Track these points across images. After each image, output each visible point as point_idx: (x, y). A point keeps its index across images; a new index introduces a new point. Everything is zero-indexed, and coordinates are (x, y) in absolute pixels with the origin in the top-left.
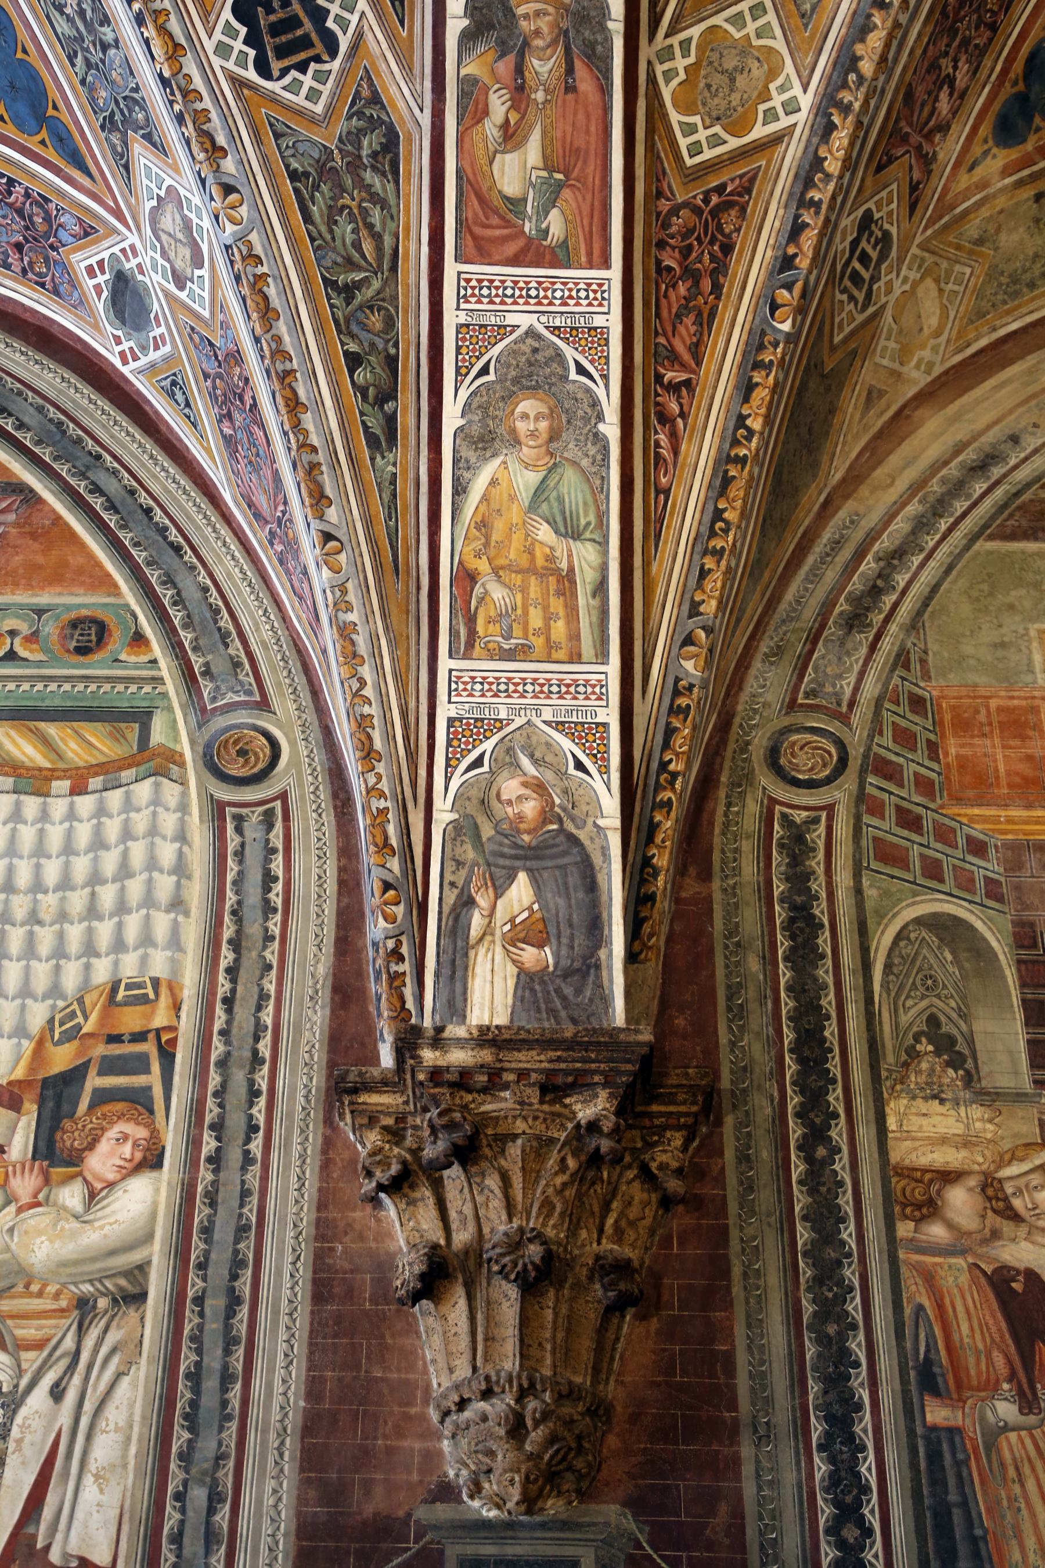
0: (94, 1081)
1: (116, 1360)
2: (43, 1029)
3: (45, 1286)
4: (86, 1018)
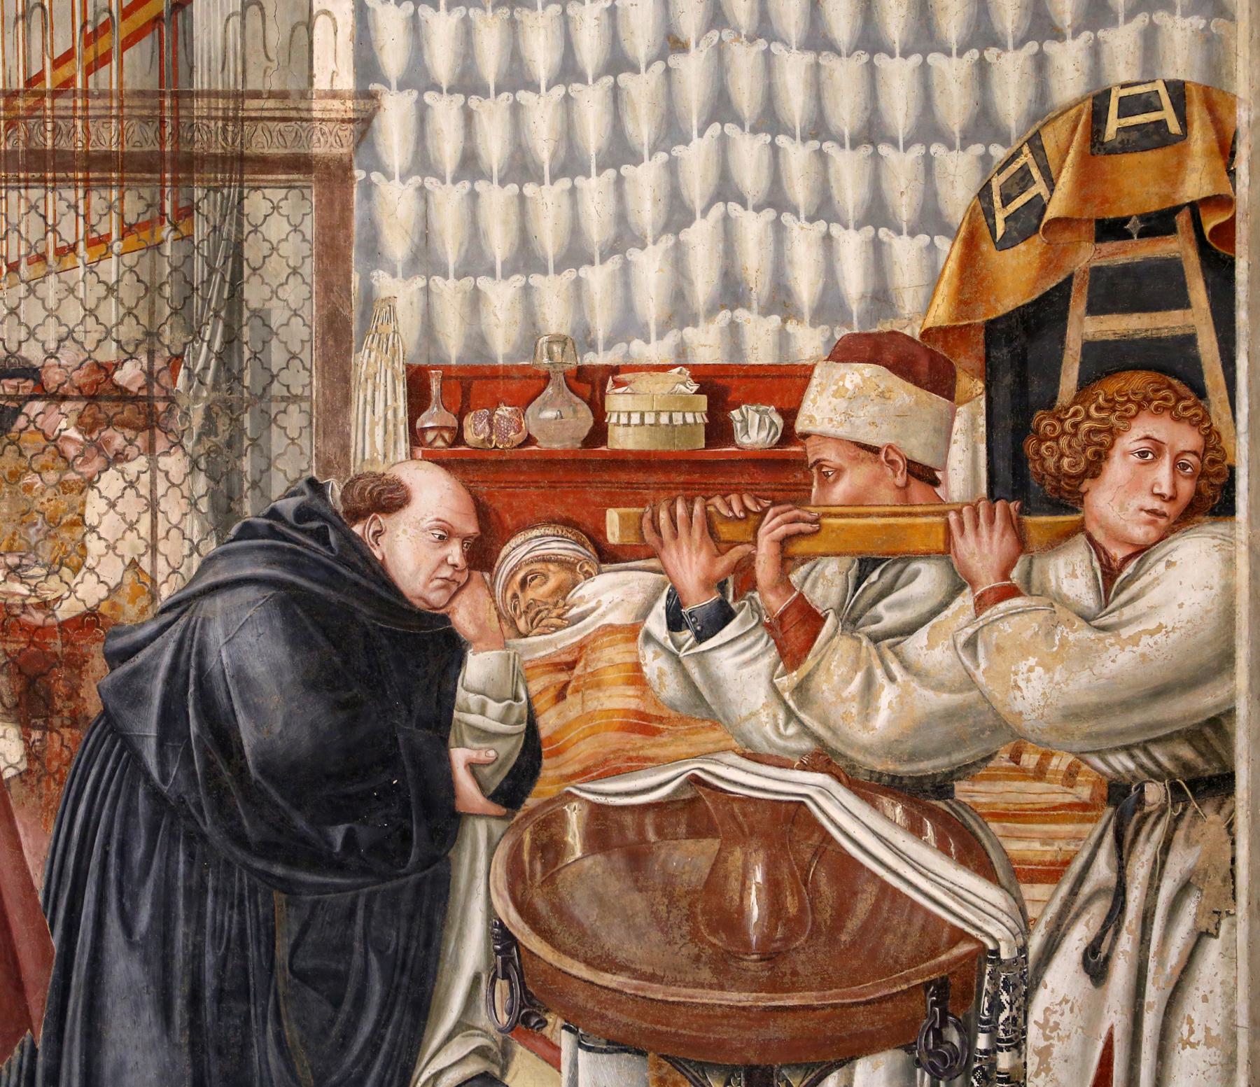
0: (1084, 327)
1: (1190, 907)
2: (972, 211)
3: (1047, 756)
4: (1051, 184)
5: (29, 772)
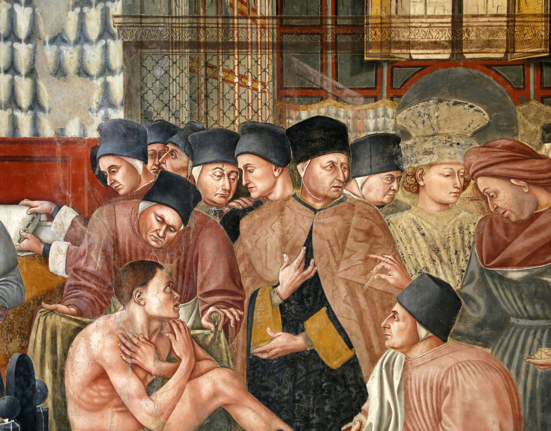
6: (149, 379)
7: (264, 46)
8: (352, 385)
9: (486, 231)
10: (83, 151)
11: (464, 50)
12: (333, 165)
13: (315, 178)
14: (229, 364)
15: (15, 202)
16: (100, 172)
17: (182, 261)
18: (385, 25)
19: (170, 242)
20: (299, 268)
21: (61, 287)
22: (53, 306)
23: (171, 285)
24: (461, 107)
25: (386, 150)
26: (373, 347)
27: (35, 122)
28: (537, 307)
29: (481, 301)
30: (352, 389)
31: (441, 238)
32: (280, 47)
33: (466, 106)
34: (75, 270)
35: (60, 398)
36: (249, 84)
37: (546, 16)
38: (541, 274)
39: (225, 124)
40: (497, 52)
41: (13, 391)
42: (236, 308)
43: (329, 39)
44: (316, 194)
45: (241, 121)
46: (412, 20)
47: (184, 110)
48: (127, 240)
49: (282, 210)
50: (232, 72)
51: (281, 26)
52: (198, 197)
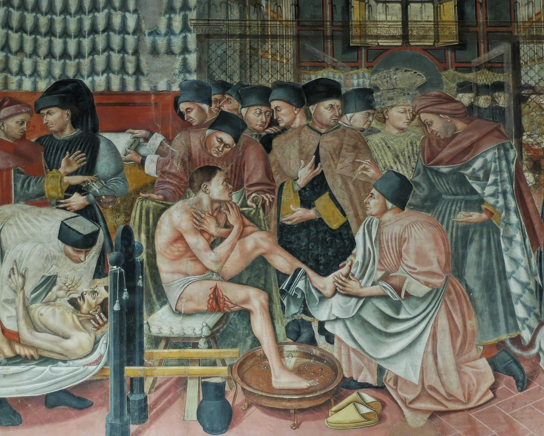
5: (535, 184)
6: (212, 239)
7: (287, 37)
8: (346, 239)
9: (426, 144)
10: (170, 99)
11: (410, 41)
12: (332, 106)
13: (321, 114)
14: (265, 228)
15: (123, 130)
16: (180, 112)
17: (234, 165)
18: (362, 25)
19: (226, 154)
20: (311, 168)
21: (153, 183)
22: (147, 195)
23: (227, 180)
24: (409, 73)
25: (365, 97)
26: (358, 215)
27: (137, 83)
28: (458, 188)
29: (424, 185)
30: (346, 241)
31: (399, 149)
32: (298, 38)
33: (412, 72)
34: (163, 172)
35: (151, 252)
36: (278, 59)
37: (456, 22)
38: (460, 169)
39: (263, 83)
40: (429, 42)
41: (120, 248)
42: (270, 194)
43: (329, 33)
44: (321, 123)
45: (273, 81)
46: (378, 23)
47: (236, 74)
48: (197, 154)
49: (300, 133)
50: (267, 52)
51: (298, 25)
52: (245, 126)
